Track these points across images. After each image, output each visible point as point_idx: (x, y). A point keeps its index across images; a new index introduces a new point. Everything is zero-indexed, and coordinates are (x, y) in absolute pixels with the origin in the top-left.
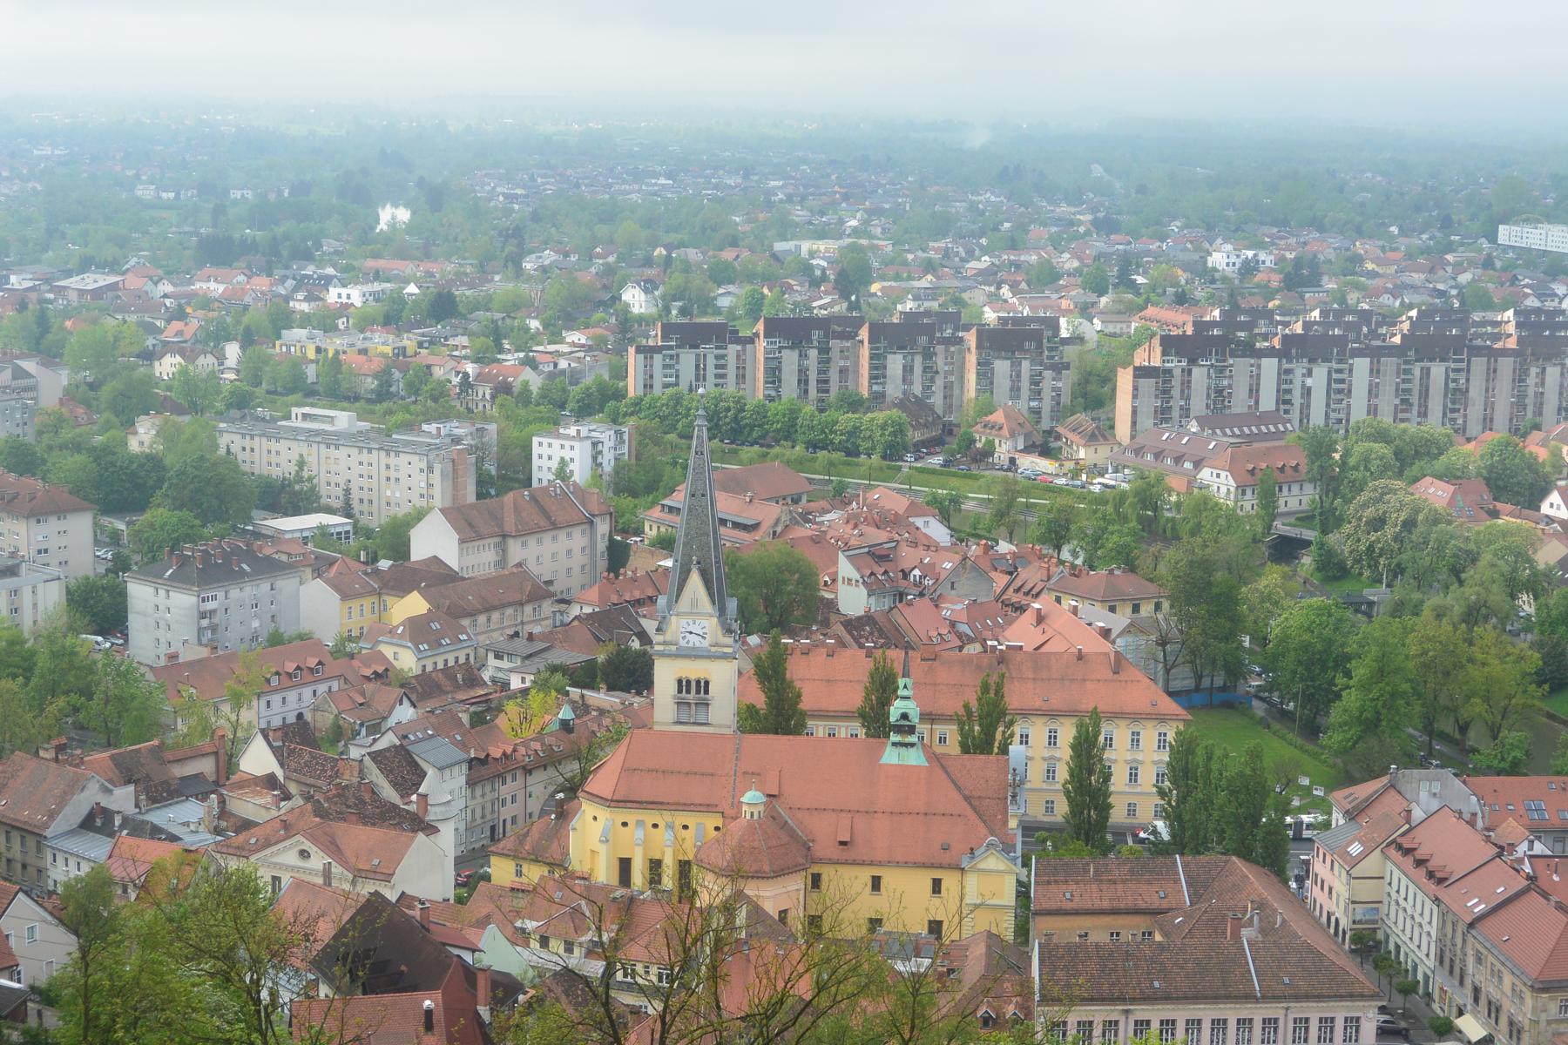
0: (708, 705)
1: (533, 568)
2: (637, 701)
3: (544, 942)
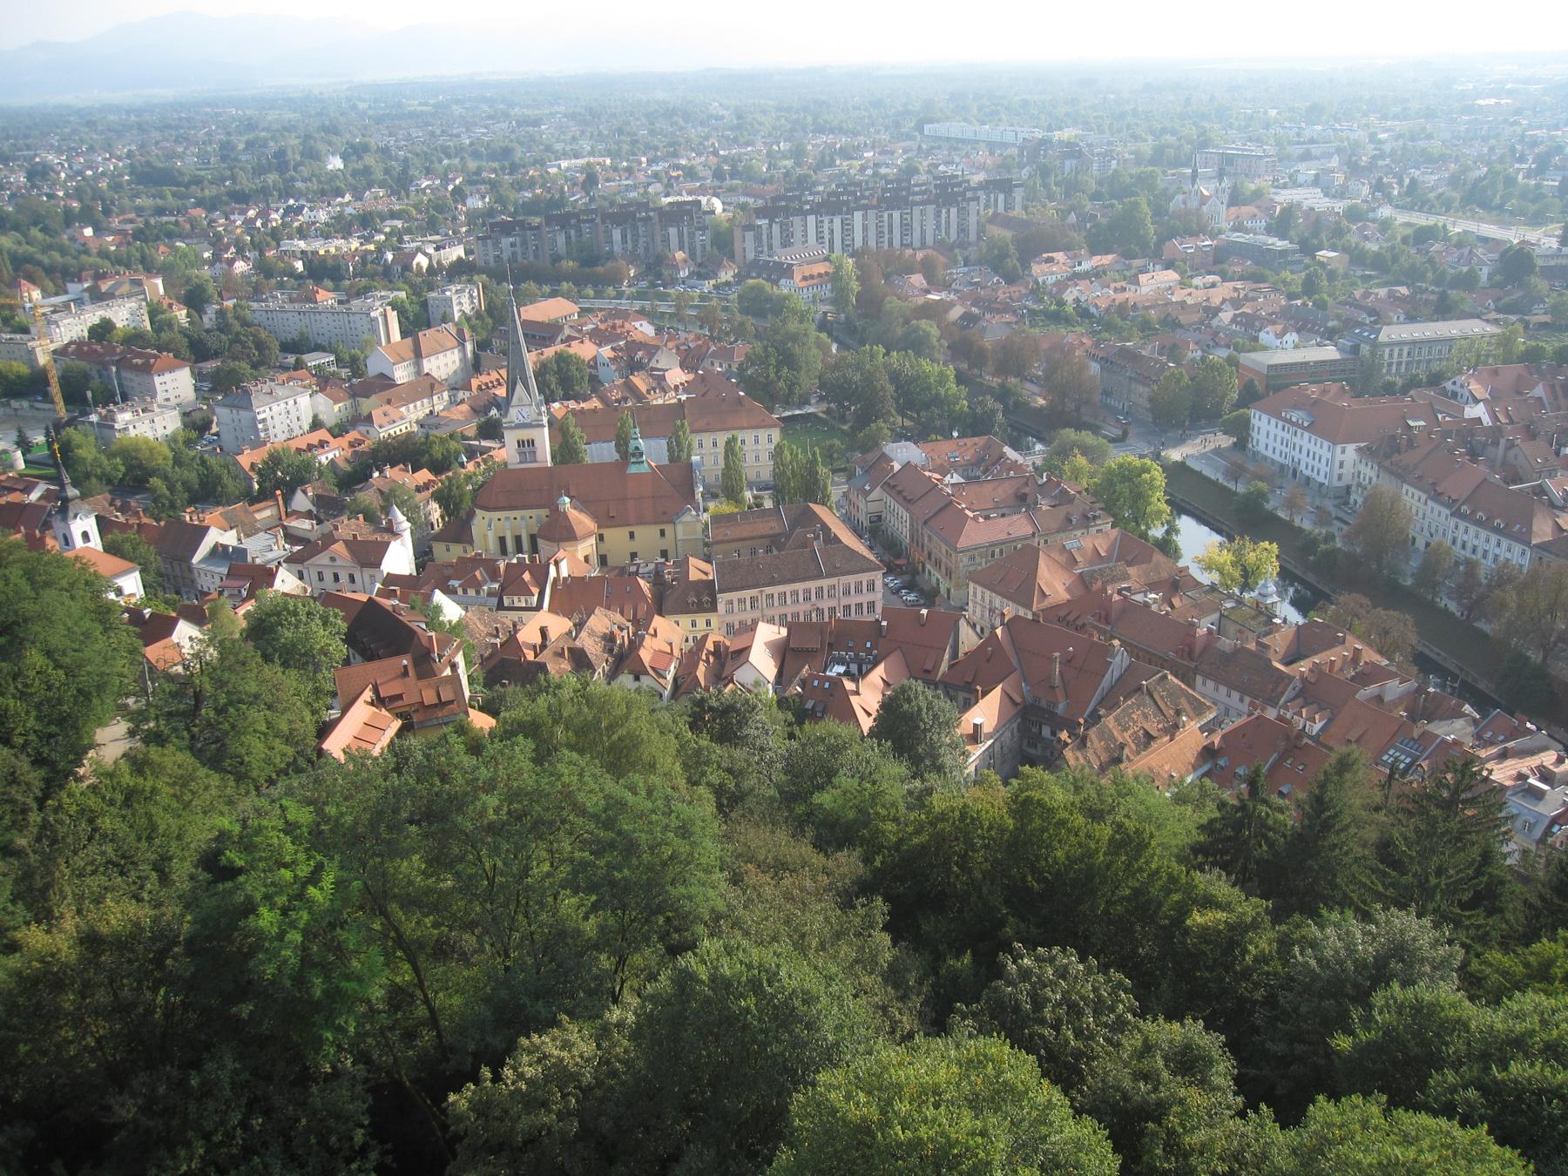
1: (435, 374)
3: (465, 592)
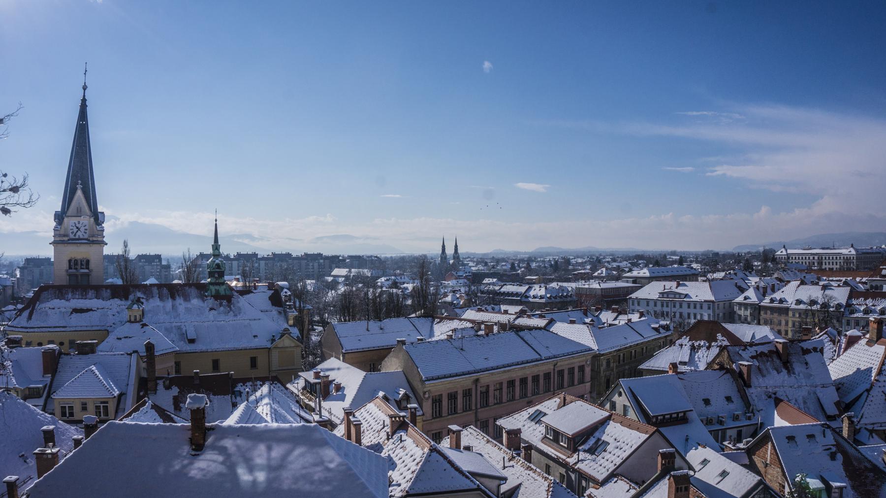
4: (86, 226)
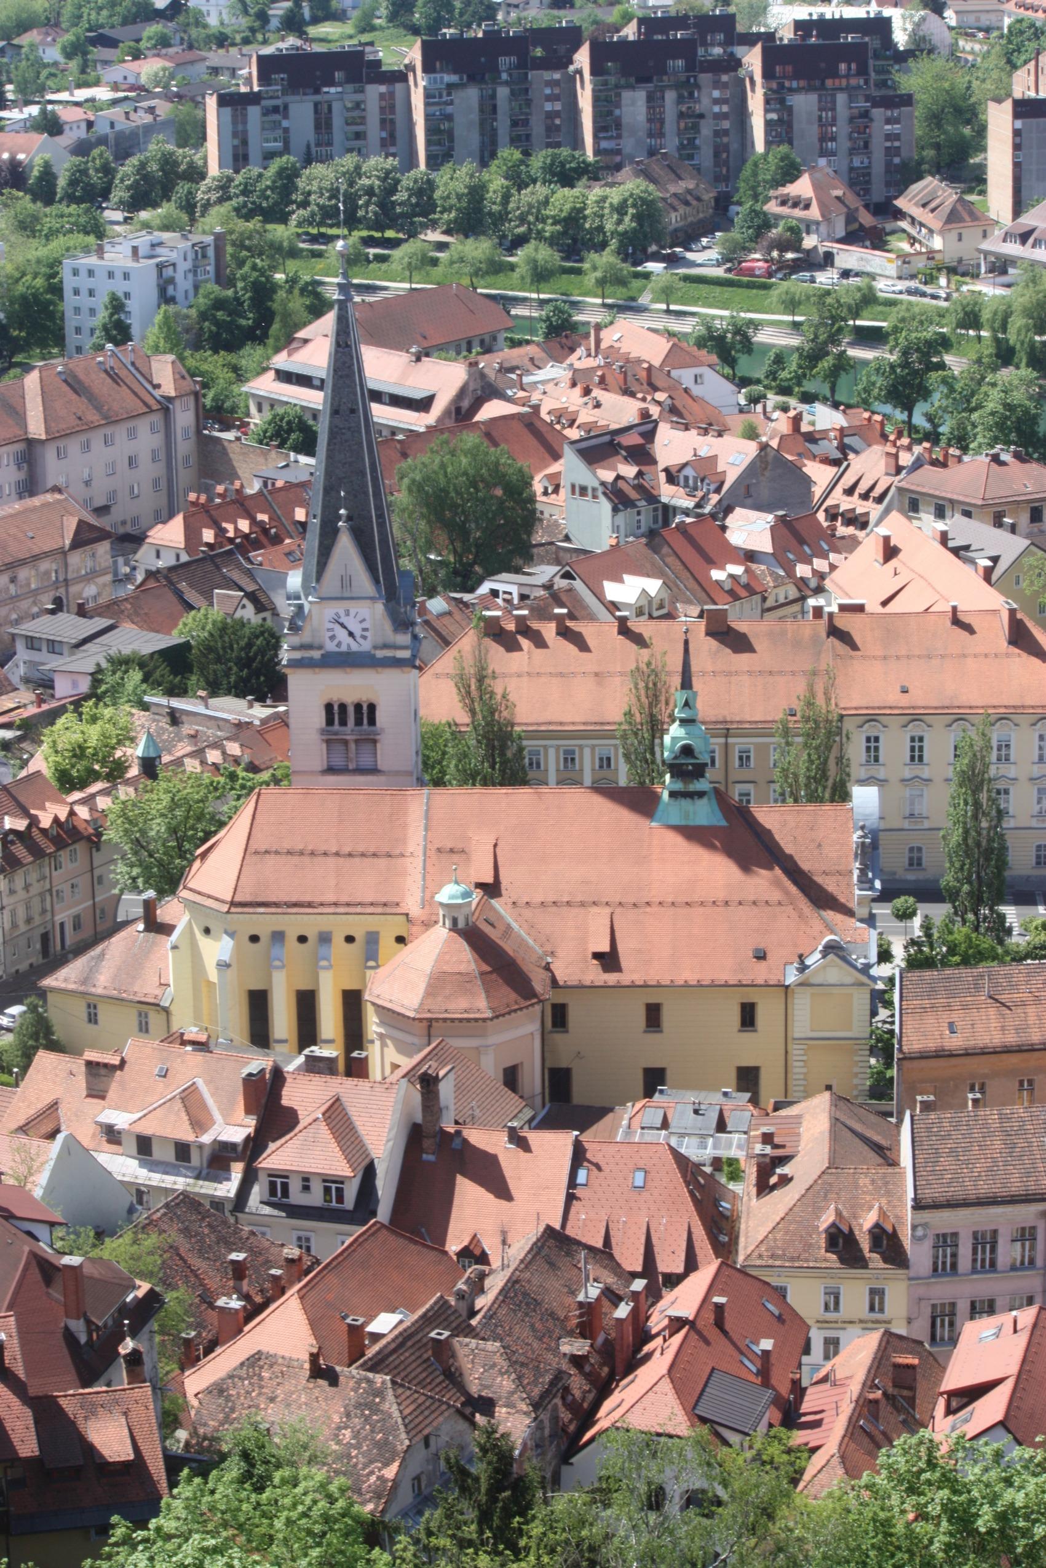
0: (375, 742)
2: (259, 712)
4: (364, 620)
